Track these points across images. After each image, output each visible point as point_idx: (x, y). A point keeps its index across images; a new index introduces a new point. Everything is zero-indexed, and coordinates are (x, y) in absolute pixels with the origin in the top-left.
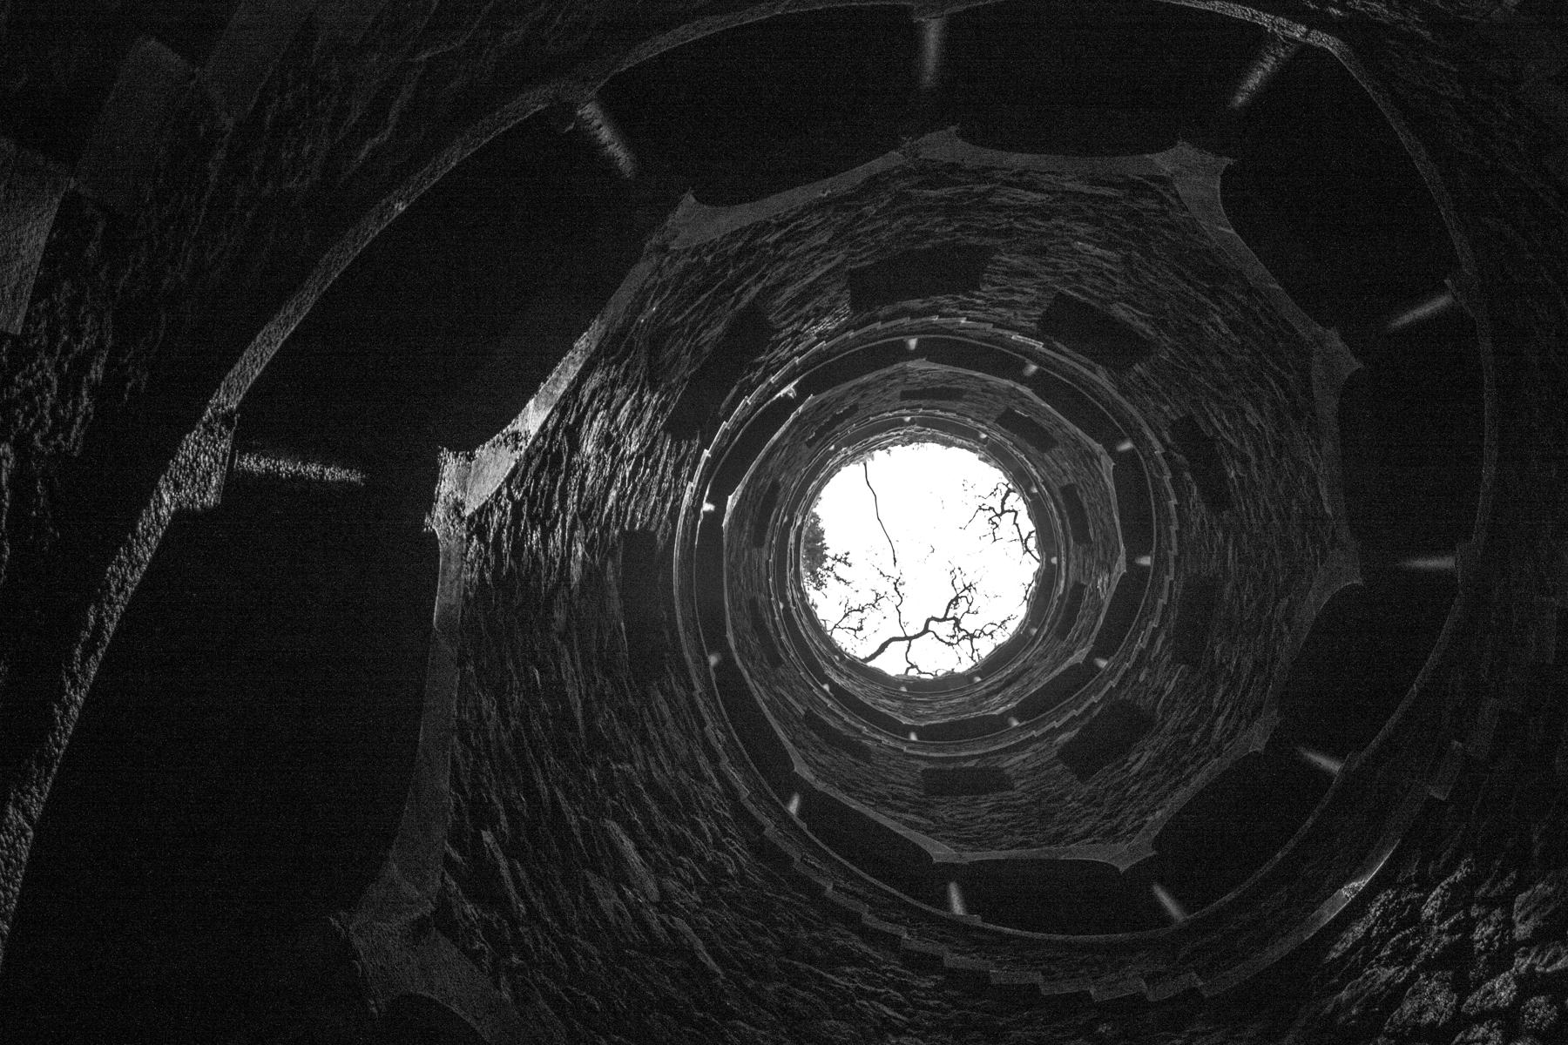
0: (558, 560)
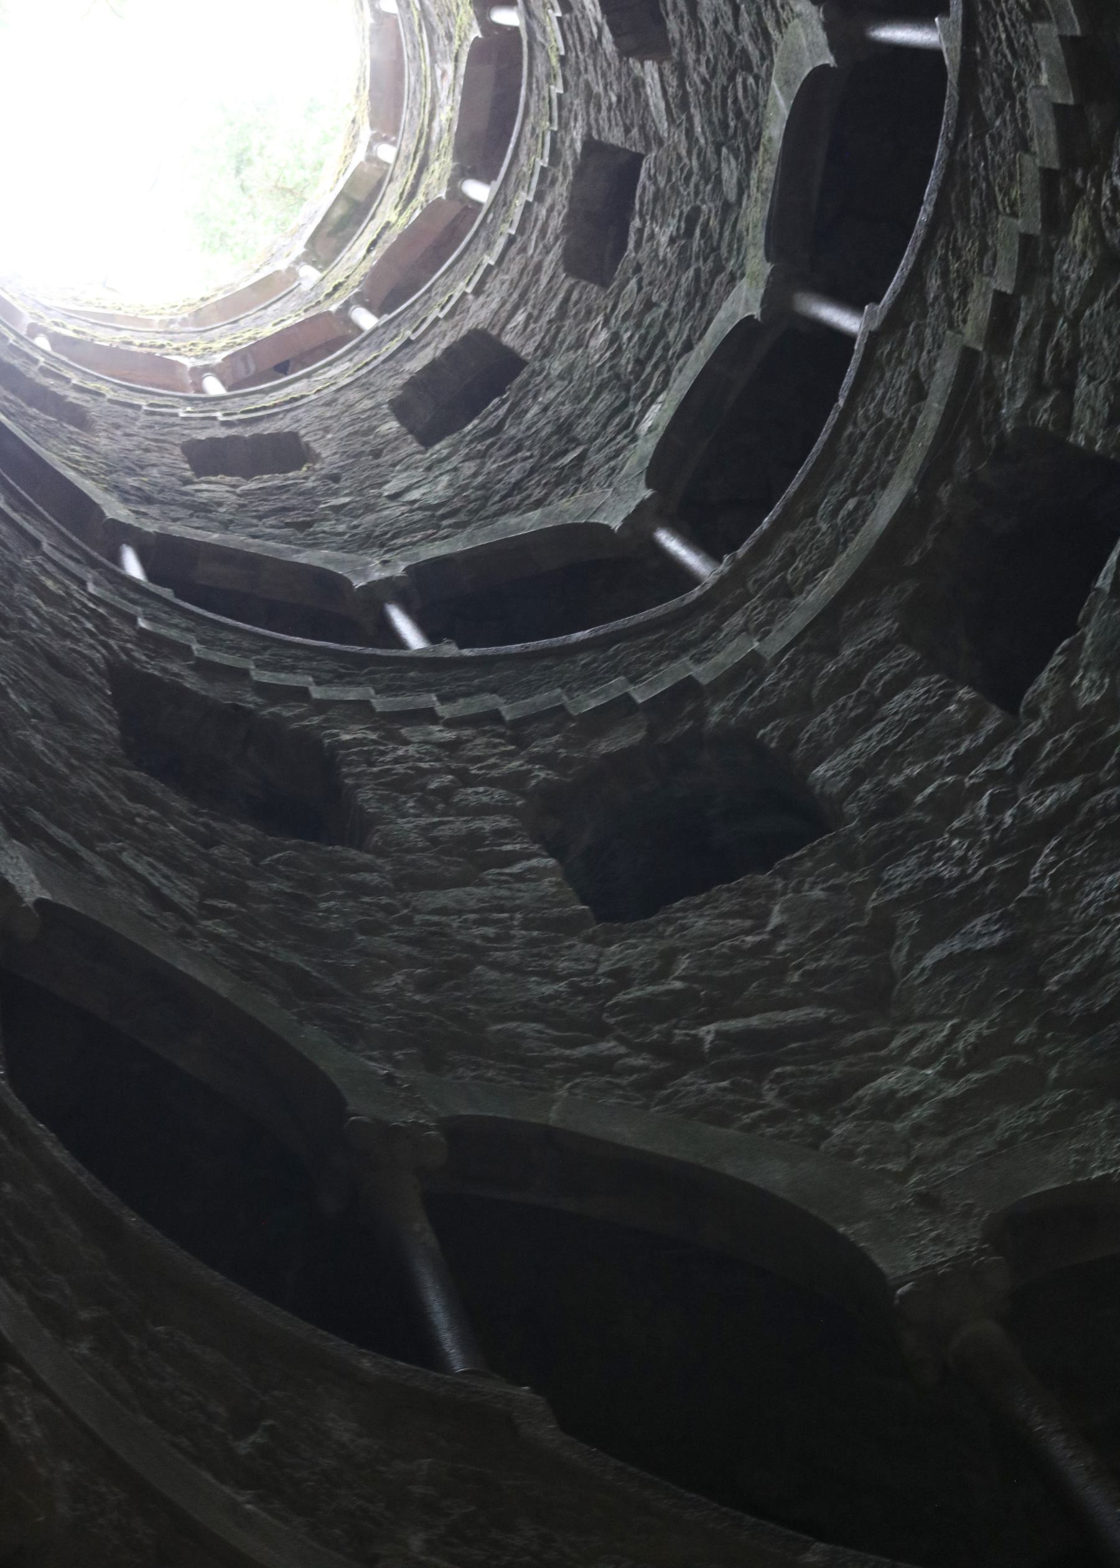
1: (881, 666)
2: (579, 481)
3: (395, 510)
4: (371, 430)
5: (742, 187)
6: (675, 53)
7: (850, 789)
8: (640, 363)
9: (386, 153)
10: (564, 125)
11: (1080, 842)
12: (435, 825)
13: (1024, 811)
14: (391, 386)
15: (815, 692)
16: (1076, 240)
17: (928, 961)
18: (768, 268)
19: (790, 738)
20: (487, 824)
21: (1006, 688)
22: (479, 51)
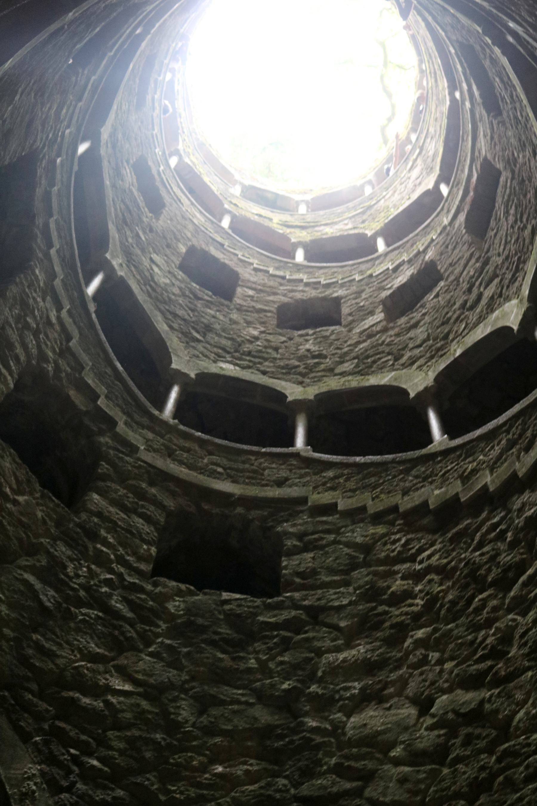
0: (145, 704)
1: (152, 508)
2: (187, 343)
3: (146, 263)
4: (178, 240)
5: (343, 374)
6: (391, 325)
7: (92, 513)
8: (249, 353)
9: (302, 209)
10: (342, 286)
11: (104, 626)
12: (11, 326)
13: (110, 596)
14: (200, 243)
15: (130, 482)
16: (372, 530)
17: (26, 576)
18: (311, 397)
19: (104, 478)
20: (19, 350)
21: (162, 568)
22: (362, 237)
